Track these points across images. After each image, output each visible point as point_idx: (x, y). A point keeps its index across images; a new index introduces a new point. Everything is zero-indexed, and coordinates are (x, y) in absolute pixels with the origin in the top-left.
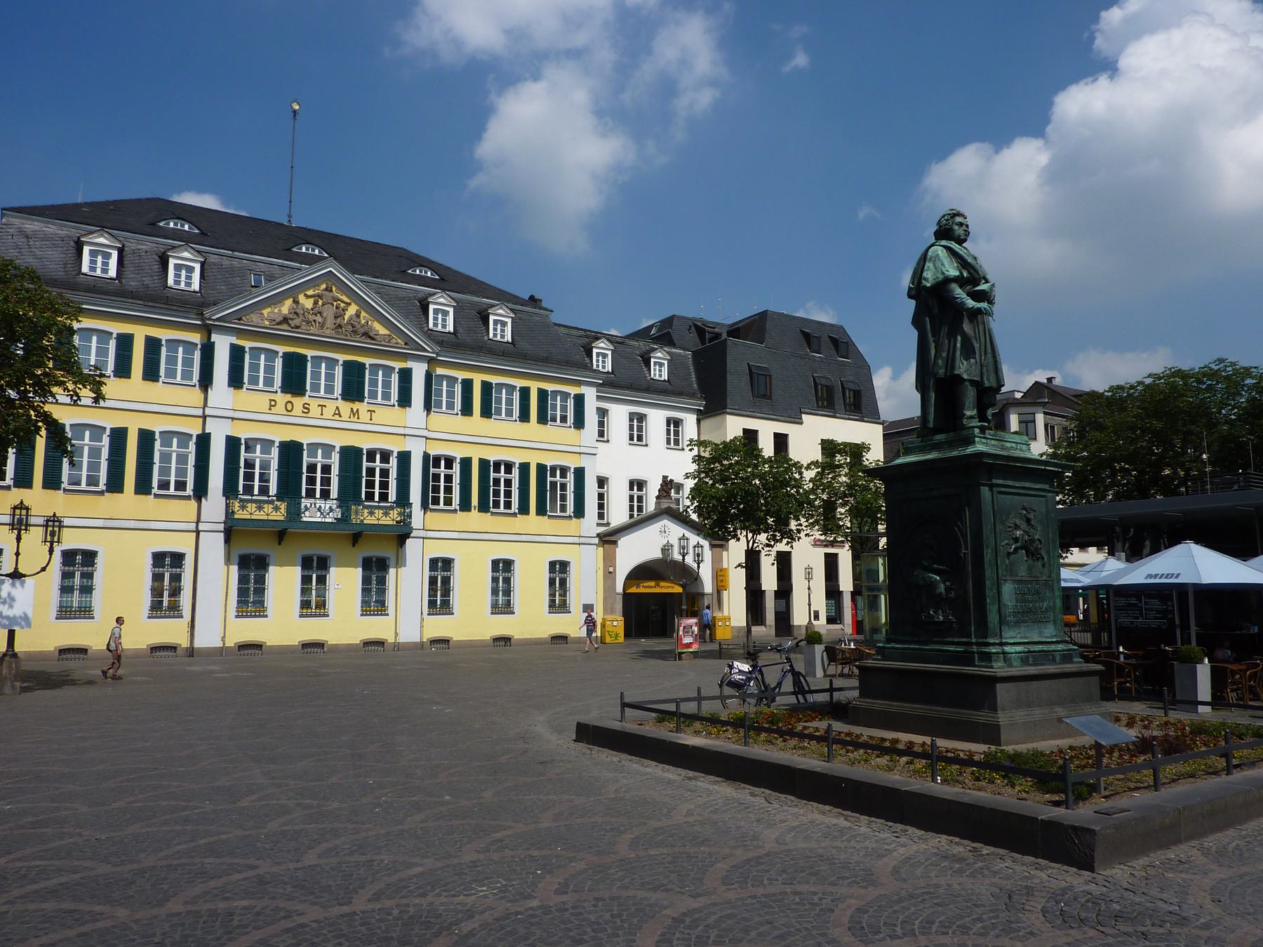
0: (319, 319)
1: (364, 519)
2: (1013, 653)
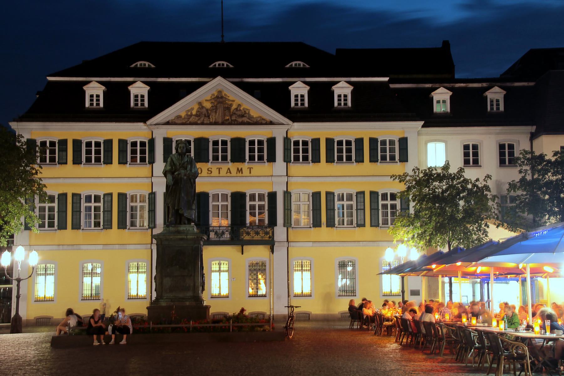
1: (244, 237)
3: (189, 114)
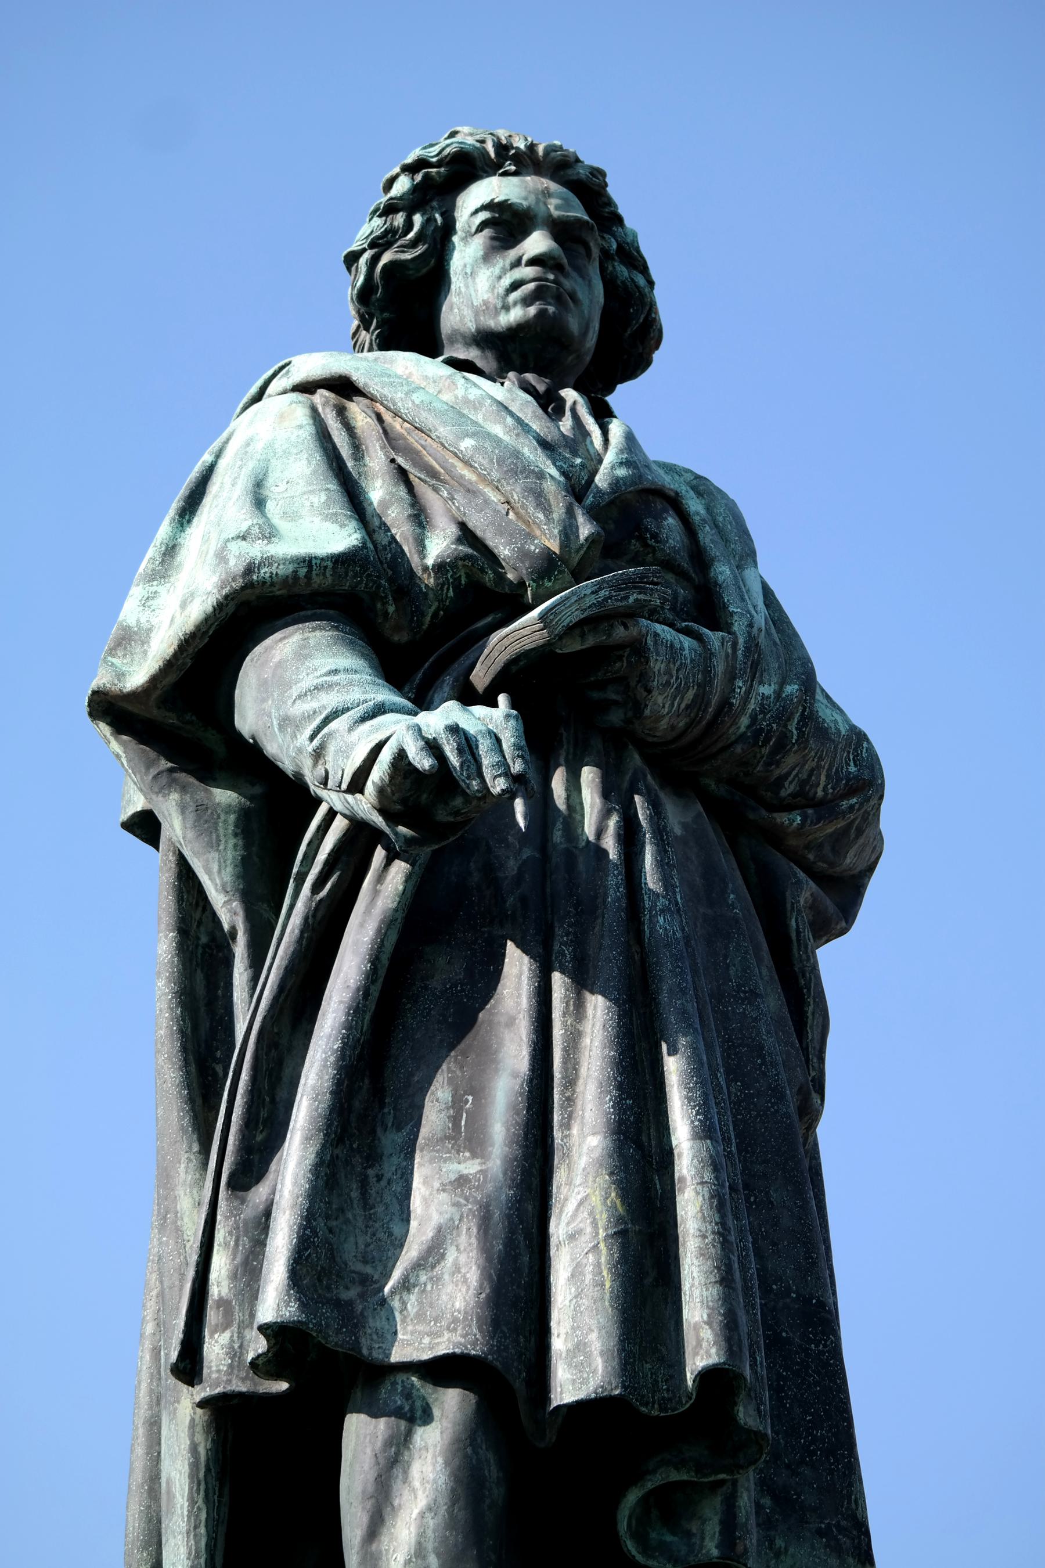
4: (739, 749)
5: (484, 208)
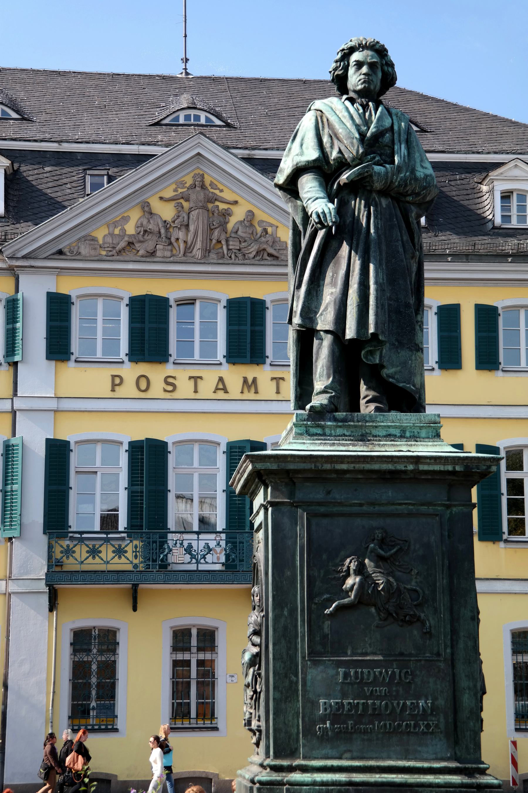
0: (181, 235)
2: (307, 785)
3: (117, 231)
4: (396, 189)
5: (355, 61)
